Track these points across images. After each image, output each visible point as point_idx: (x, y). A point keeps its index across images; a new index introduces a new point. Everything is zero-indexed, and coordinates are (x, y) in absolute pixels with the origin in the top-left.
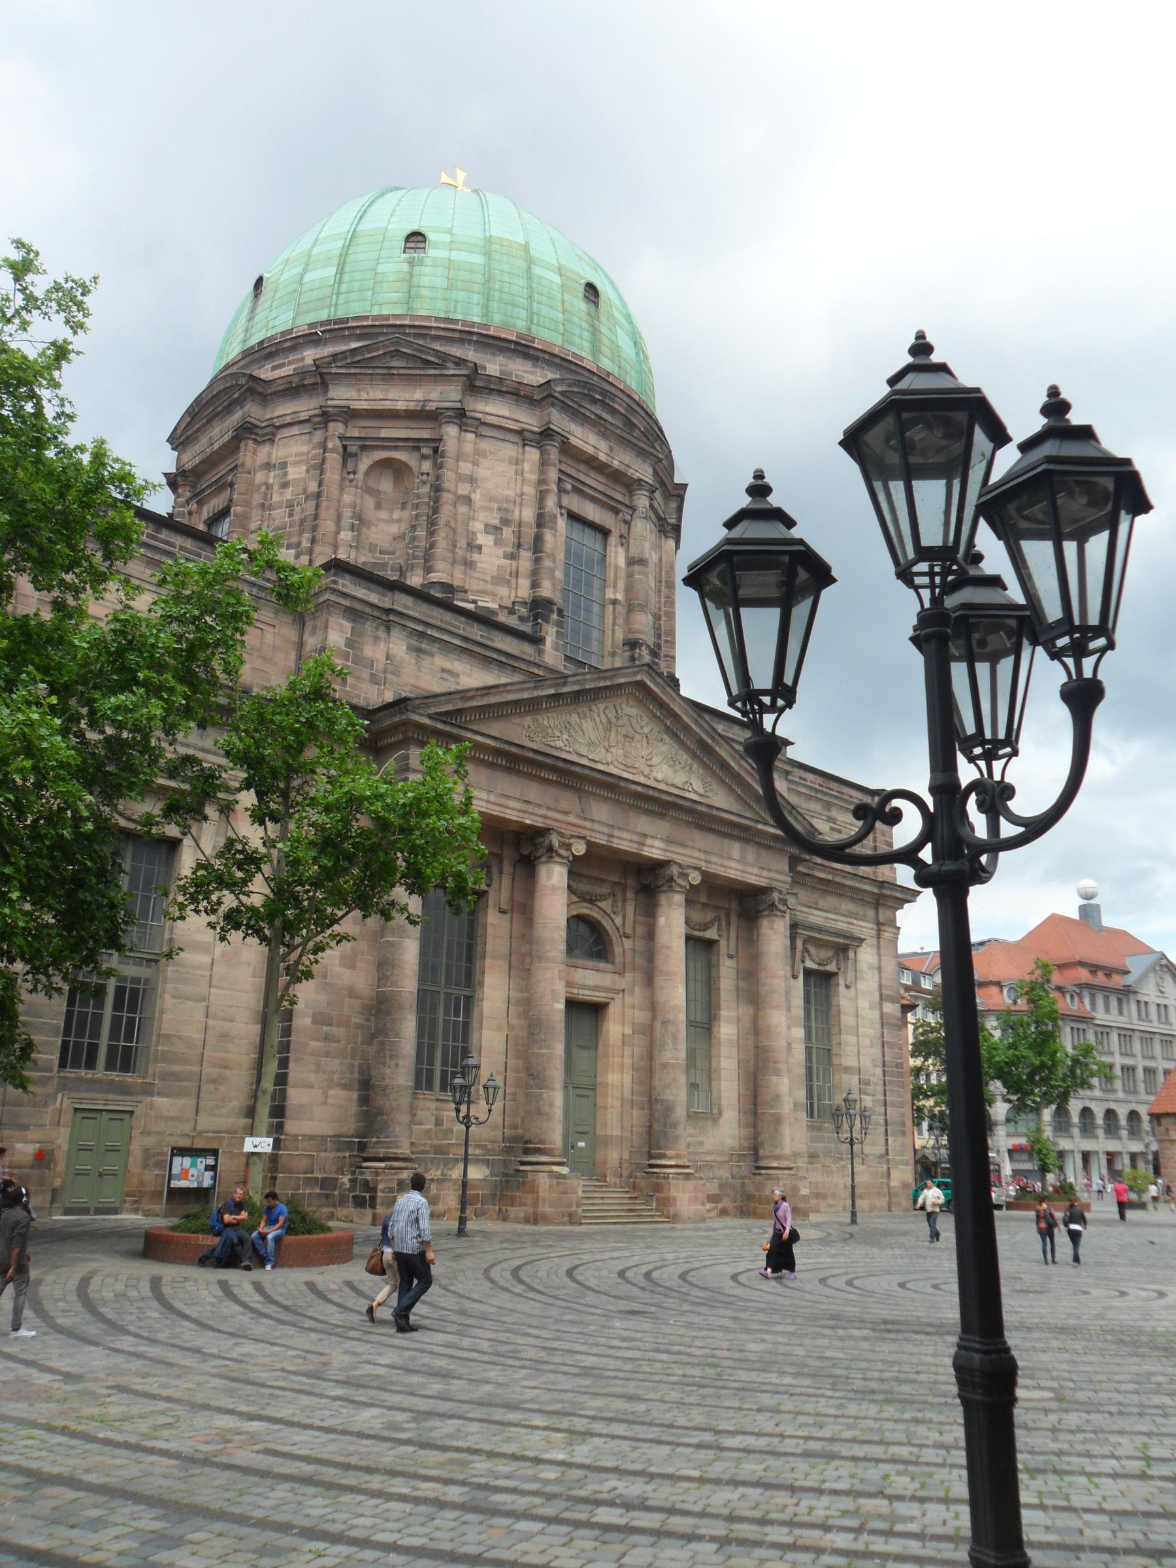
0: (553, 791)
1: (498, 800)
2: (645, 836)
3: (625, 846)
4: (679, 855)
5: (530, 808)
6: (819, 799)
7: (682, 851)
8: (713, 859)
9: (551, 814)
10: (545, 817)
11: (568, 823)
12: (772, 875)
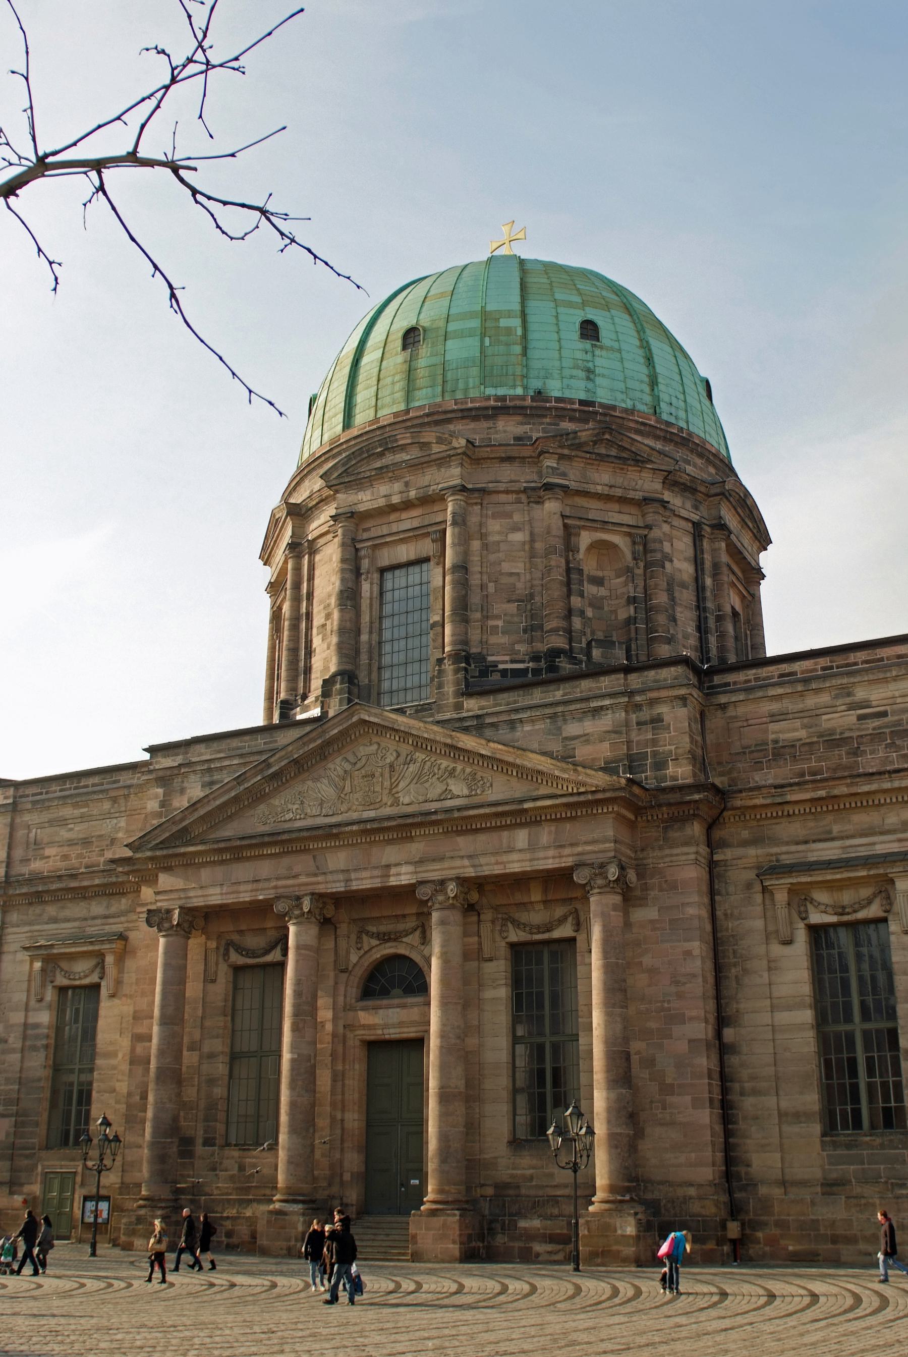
0: (286, 861)
1: (230, 890)
2: (388, 866)
3: (367, 884)
4: (434, 872)
5: (261, 885)
6: (818, 691)
7: (437, 866)
8: (483, 860)
9: (280, 883)
10: (276, 887)
11: (299, 885)
12: (580, 849)
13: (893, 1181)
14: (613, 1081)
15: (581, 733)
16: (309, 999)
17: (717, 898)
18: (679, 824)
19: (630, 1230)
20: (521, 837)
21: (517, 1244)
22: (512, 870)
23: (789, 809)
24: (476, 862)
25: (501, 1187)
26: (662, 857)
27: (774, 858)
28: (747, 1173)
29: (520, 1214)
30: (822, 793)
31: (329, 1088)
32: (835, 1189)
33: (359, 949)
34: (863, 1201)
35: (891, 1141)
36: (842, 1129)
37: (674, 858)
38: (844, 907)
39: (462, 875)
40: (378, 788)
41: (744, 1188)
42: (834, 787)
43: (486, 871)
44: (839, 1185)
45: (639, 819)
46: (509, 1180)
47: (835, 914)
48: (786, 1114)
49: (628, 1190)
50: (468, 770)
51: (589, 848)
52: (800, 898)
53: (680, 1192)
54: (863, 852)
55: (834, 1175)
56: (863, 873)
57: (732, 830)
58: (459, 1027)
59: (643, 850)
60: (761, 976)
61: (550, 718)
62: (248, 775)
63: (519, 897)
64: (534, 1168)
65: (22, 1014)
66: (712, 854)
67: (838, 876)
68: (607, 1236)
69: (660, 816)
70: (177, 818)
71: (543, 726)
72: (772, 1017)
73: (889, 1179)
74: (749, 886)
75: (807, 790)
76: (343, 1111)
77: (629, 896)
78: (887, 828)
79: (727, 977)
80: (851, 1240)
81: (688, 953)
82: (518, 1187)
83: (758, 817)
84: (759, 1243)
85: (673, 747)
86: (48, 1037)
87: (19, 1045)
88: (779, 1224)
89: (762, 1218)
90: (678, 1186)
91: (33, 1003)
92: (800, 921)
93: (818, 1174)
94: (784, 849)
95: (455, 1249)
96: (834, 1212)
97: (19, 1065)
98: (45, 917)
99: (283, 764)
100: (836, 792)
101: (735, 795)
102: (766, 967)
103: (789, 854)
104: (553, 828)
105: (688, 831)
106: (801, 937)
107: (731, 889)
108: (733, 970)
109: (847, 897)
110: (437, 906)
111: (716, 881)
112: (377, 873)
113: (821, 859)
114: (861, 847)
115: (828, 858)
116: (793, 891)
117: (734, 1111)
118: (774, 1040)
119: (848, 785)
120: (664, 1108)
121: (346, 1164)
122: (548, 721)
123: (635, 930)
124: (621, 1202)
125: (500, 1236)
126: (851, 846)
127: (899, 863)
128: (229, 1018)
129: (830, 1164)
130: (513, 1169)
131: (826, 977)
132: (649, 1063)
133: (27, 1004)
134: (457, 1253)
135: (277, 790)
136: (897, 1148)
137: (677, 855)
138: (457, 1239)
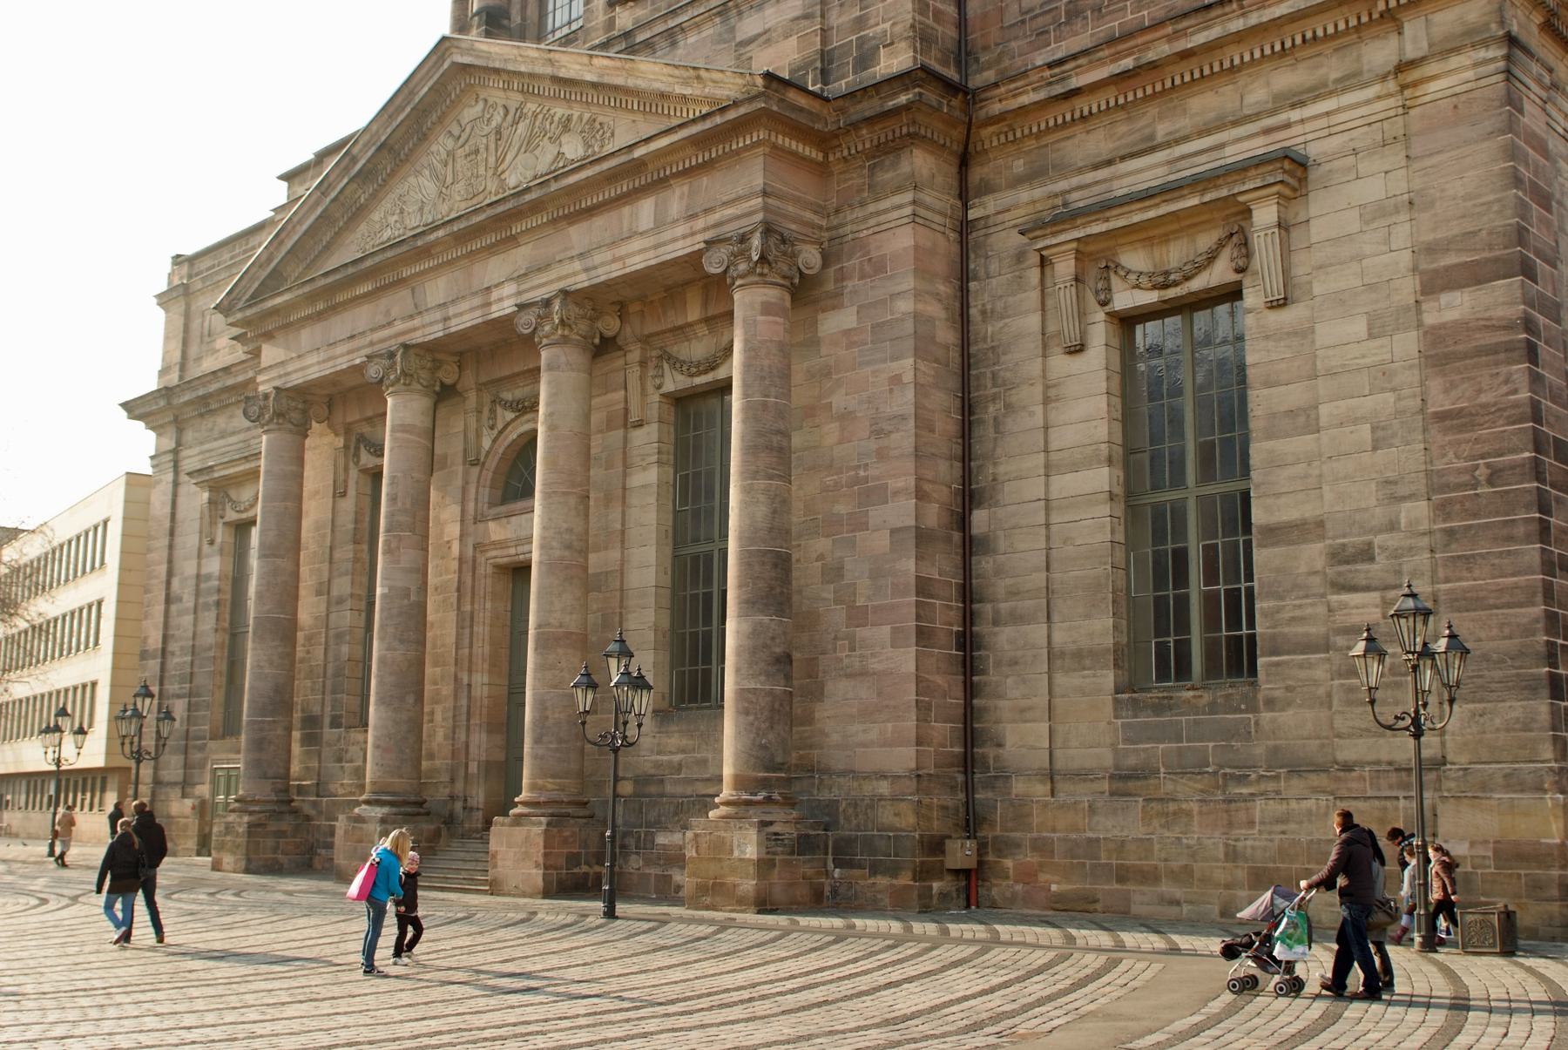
8: (598, 258)
12: (716, 217)
13: (1228, 770)
14: (747, 602)
15: (760, 30)
16: (408, 506)
17: (973, 285)
18: (891, 157)
19: (751, 851)
20: (645, 210)
21: (653, 871)
22: (633, 269)
23: (1083, 105)
24: (589, 262)
25: (642, 781)
26: (865, 219)
27: (1059, 201)
28: (997, 758)
29: (659, 825)
30: (1128, 63)
31: (453, 639)
32: (1131, 785)
33: (492, 428)
34: (1172, 807)
35: (1227, 697)
36: (1159, 679)
37: (882, 218)
38: (1167, 273)
39: (573, 288)
40: (482, 171)
41: (990, 784)
42: (1146, 46)
43: (605, 273)
44: (1138, 778)
45: (831, 158)
46: (652, 771)
47: (1154, 287)
48: (1063, 654)
49: (764, 784)
50: (587, 116)
51: (730, 212)
52: (1097, 262)
53: (868, 788)
54: (1204, 165)
55: (1131, 761)
56: (1194, 201)
57: (997, 165)
58: (569, 530)
59: (837, 211)
60: (1031, 414)
61: (719, 14)
62: (331, 178)
63: (674, 319)
64: (683, 751)
65: (195, 562)
66: (966, 207)
67: (1152, 214)
68: (720, 860)
69: (860, 148)
70: (264, 258)
71: (711, 31)
72: (1047, 485)
73: (1222, 767)
74: (1020, 257)
75: (1101, 62)
76: (470, 671)
77: (804, 293)
78: (1247, 112)
79: (981, 422)
80: (1149, 876)
81: (896, 380)
82: (662, 781)
83: (1035, 130)
84: (1007, 878)
85: (887, 25)
86: (219, 591)
87: (191, 604)
88: (1042, 846)
89: (1013, 834)
90: (864, 778)
91: (206, 548)
92: (1098, 307)
93: (1108, 760)
94: (1075, 181)
95: (537, 876)
96: (1123, 825)
97: (191, 629)
98: (216, 434)
99: (369, 154)
100: (1151, 56)
101: (989, 94)
102: (1040, 398)
103: (1080, 188)
104: (686, 188)
105: (905, 167)
106: (1100, 333)
107: (994, 267)
108: (991, 409)
109: (1175, 254)
110: (545, 341)
111: (972, 256)
112: (477, 301)
113: (1134, 189)
114: (1198, 154)
115: (1145, 186)
116: (1084, 253)
117: (982, 653)
118: (1047, 525)
119: (1170, 38)
120: (853, 649)
121: (473, 750)
122: (718, 20)
123: (824, 351)
124: (748, 803)
125: (633, 857)
126: (1183, 157)
127: (1253, 172)
128: (365, 547)
129: (1127, 740)
130: (659, 753)
131: (1145, 408)
132: (834, 573)
133: (200, 550)
134: (540, 882)
135: (375, 197)
136: (1238, 710)
137: (886, 211)
138: (541, 860)
